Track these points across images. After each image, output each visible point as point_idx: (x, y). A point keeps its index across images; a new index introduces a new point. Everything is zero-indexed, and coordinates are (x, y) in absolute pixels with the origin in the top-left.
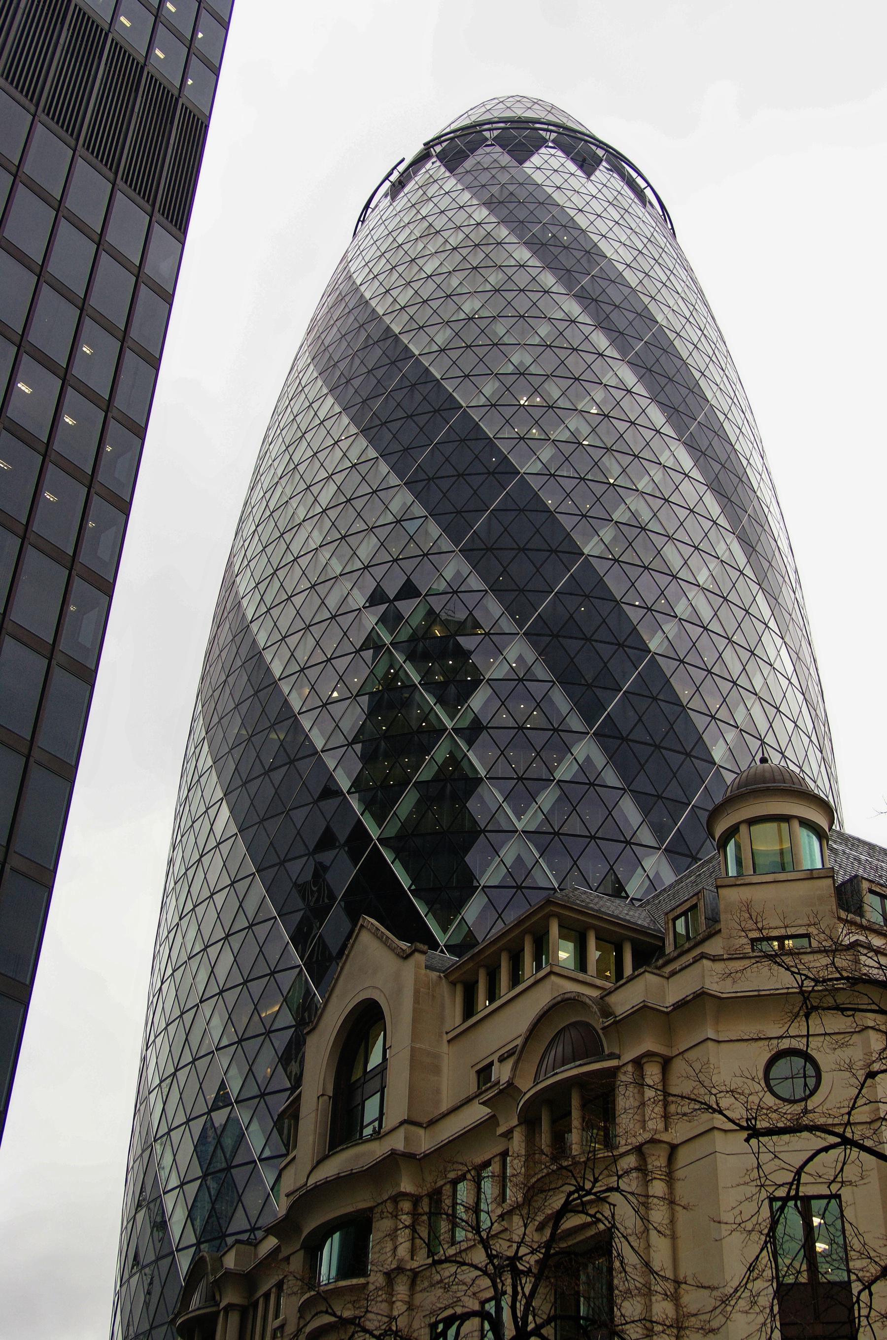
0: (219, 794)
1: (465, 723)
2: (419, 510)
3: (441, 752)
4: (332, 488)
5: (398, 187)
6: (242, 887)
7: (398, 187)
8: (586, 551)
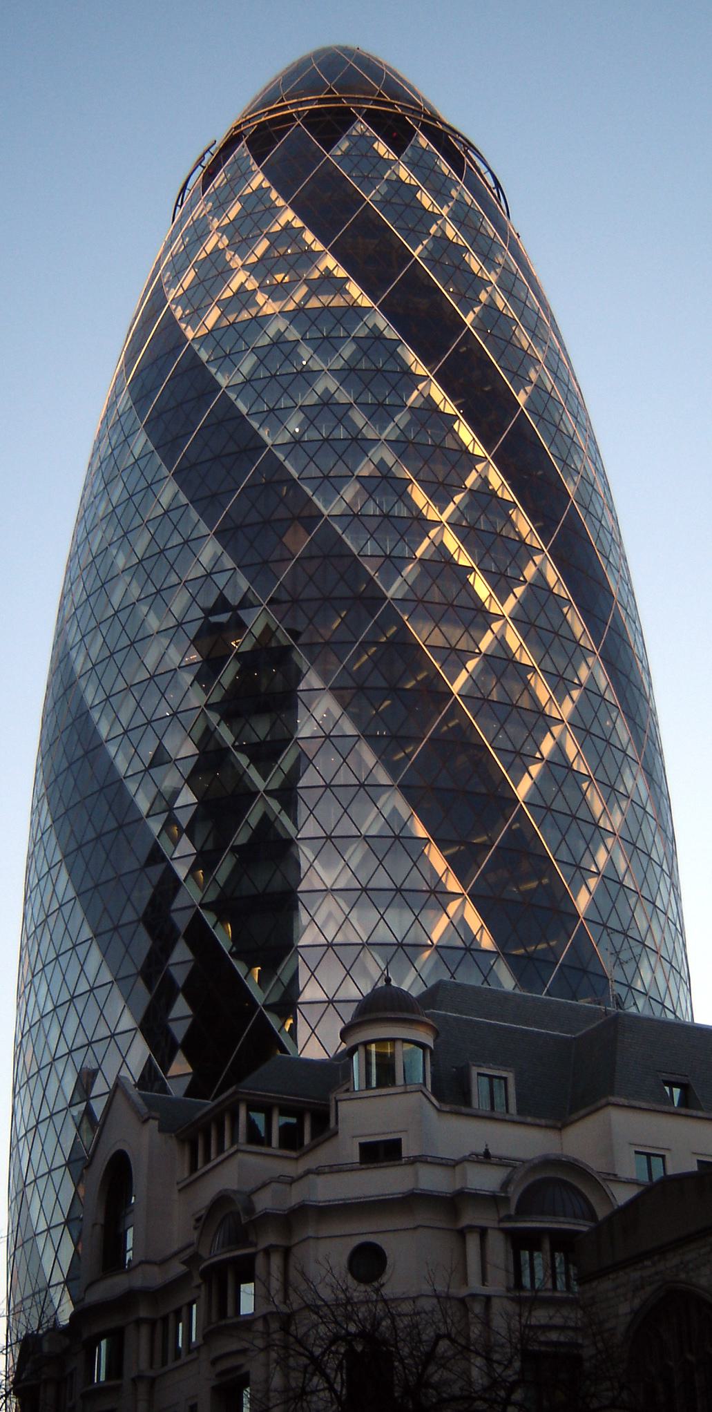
0: (58, 857)
1: (275, 785)
2: (228, 563)
3: (254, 816)
4: (147, 537)
5: (210, 175)
6: (81, 950)
7: (210, 175)
8: (389, 594)
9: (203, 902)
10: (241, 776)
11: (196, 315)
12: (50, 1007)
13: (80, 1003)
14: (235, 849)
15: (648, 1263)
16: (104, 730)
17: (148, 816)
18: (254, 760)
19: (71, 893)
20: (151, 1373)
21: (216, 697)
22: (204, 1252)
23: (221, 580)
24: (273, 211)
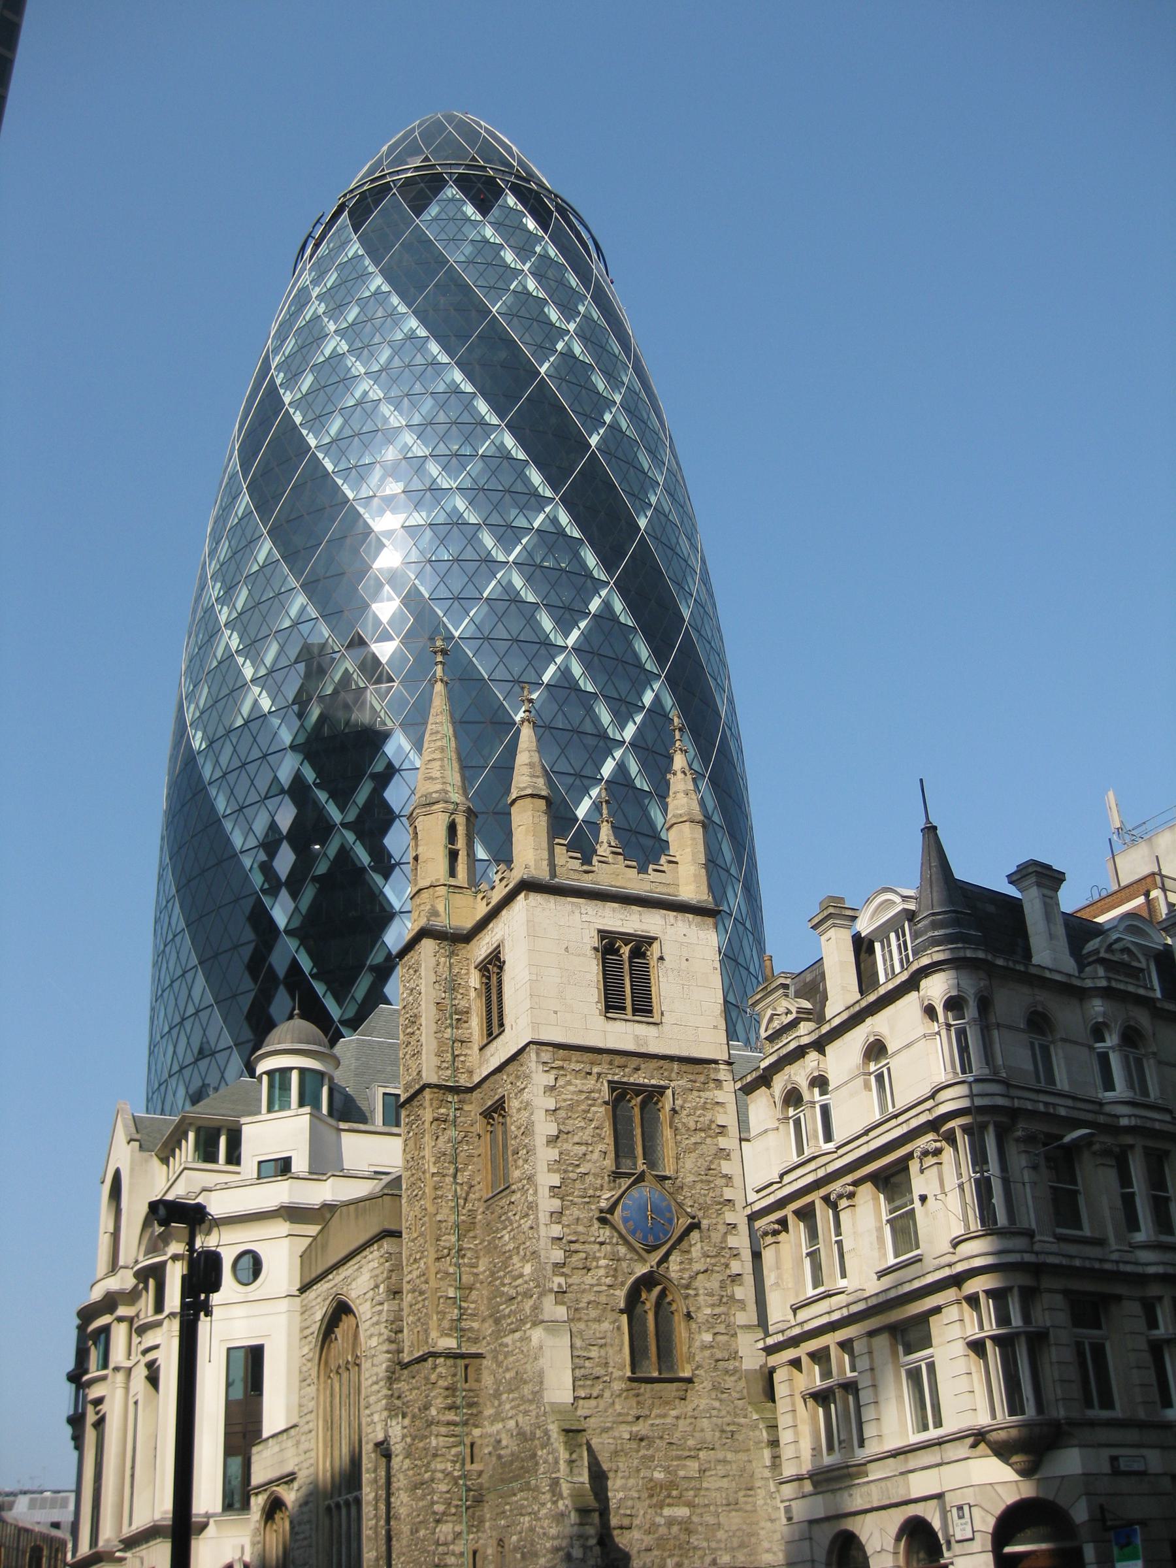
2: (312, 612)
6: (190, 975)
8: (457, 634)
9: (289, 928)
10: (320, 811)
11: (293, 379)
12: (166, 1029)
13: (188, 1024)
14: (315, 879)
15: (330, 1277)
16: (207, 773)
17: (241, 852)
18: (333, 796)
19: (182, 924)
20: (128, 1364)
21: (301, 740)
22: (141, 1258)
23: (305, 628)
24: (364, 276)
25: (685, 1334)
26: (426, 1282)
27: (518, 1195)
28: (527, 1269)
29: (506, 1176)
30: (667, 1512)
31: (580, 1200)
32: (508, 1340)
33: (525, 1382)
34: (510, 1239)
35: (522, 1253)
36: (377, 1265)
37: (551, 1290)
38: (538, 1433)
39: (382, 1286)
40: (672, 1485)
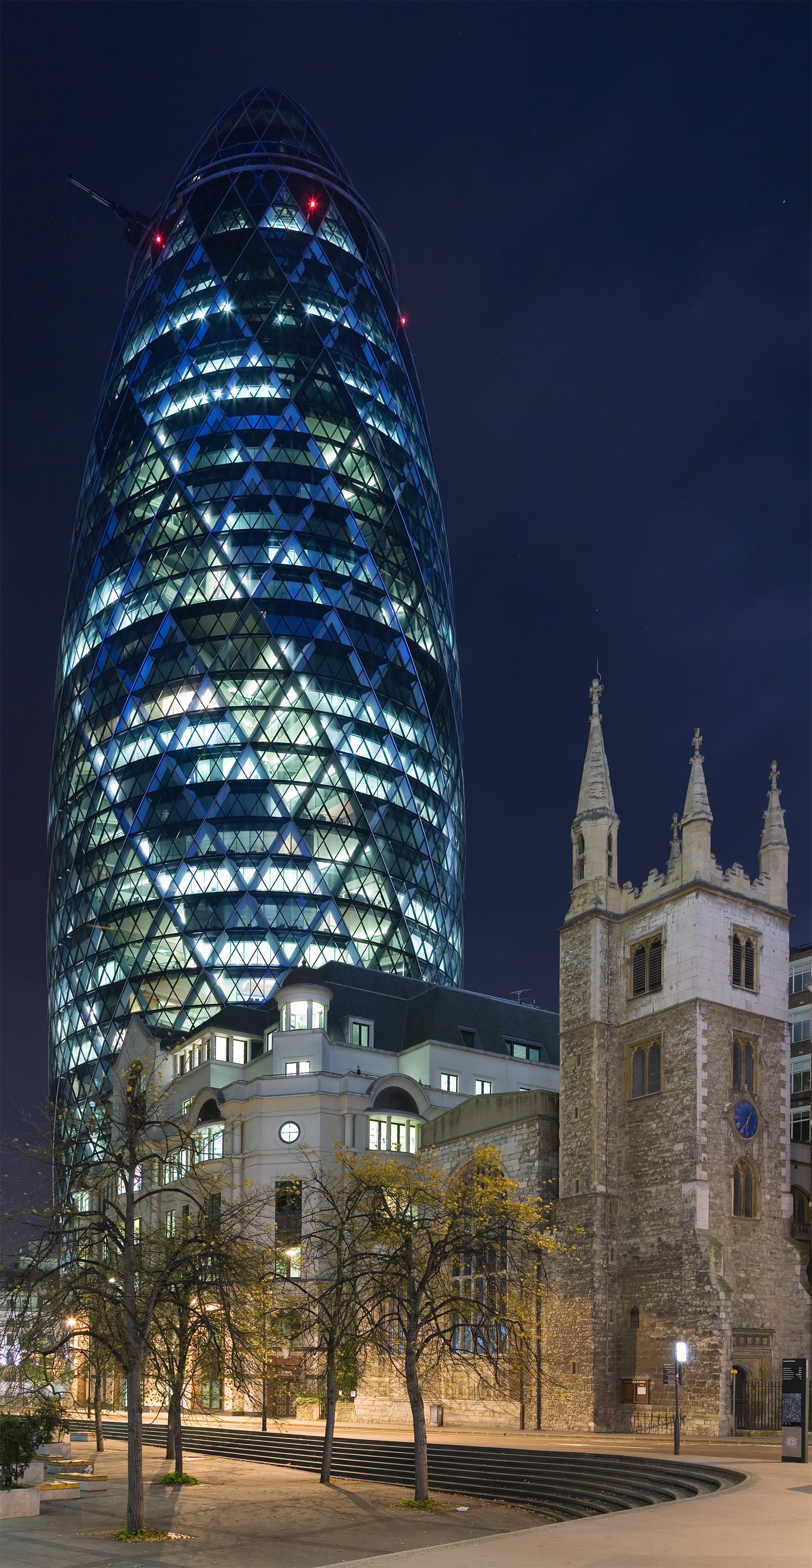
25: (758, 1194)
26: (588, 1150)
27: (671, 1100)
28: (679, 1147)
29: (656, 1086)
30: (745, 1296)
31: (715, 1107)
32: (653, 1190)
33: (671, 1215)
34: (658, 1127)
35: (671, 1136)
36: (525, 1136)
37: (700, 1161)
38: (684, 1246)
39: (532, 1152)
40: (747, 1281)
